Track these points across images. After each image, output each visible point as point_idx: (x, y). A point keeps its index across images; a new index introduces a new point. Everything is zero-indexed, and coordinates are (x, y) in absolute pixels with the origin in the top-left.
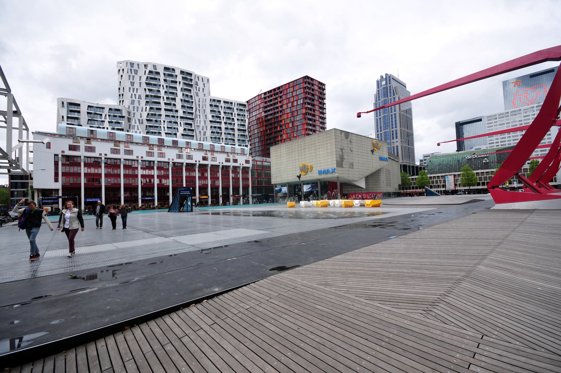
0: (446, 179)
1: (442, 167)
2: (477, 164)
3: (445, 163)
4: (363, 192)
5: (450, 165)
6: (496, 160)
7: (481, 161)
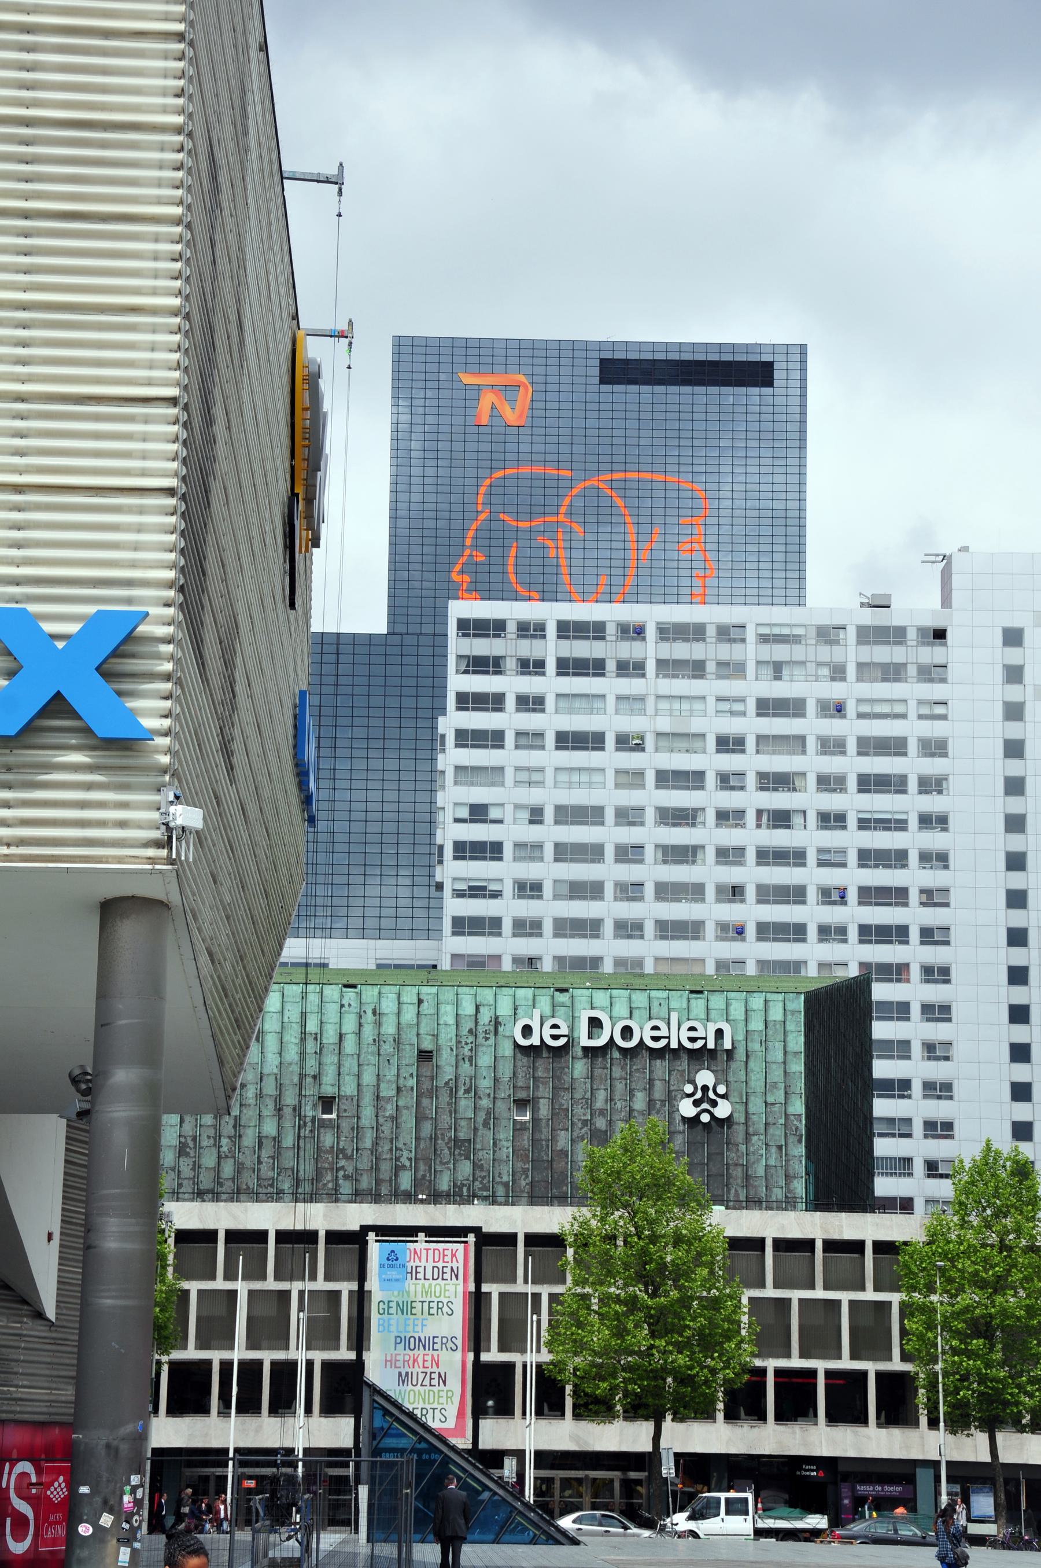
0: (373, 1284)
3: (272, 1061)
6: (798, 1106)
7: (659, 1092)
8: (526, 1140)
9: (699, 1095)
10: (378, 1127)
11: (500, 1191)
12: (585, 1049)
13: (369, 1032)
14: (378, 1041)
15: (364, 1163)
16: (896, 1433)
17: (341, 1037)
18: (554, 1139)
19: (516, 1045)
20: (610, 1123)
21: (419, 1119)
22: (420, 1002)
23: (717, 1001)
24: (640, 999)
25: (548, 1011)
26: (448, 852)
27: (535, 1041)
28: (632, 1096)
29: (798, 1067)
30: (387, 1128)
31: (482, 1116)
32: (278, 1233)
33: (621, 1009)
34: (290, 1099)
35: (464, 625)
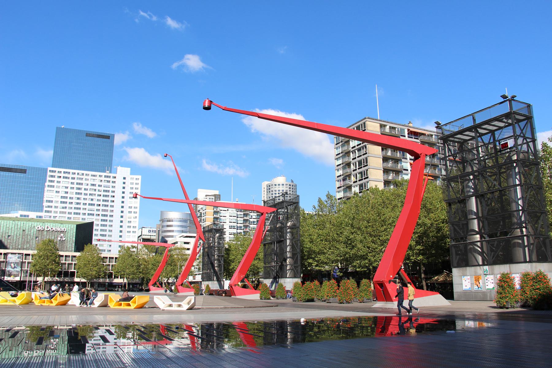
8: (37, 242)
11: (33, 248)
13: (16, 227)
14: (17, 228)
15: (14, 244)
21: (22, 239)
23: (65, 225)
24: (54, 224)
25: (41, 226)
26: (45, 201)
29: (75, 234)
30: (17, 240)
31: (31, 239)
33: (52, 226)
35: (50, 171)
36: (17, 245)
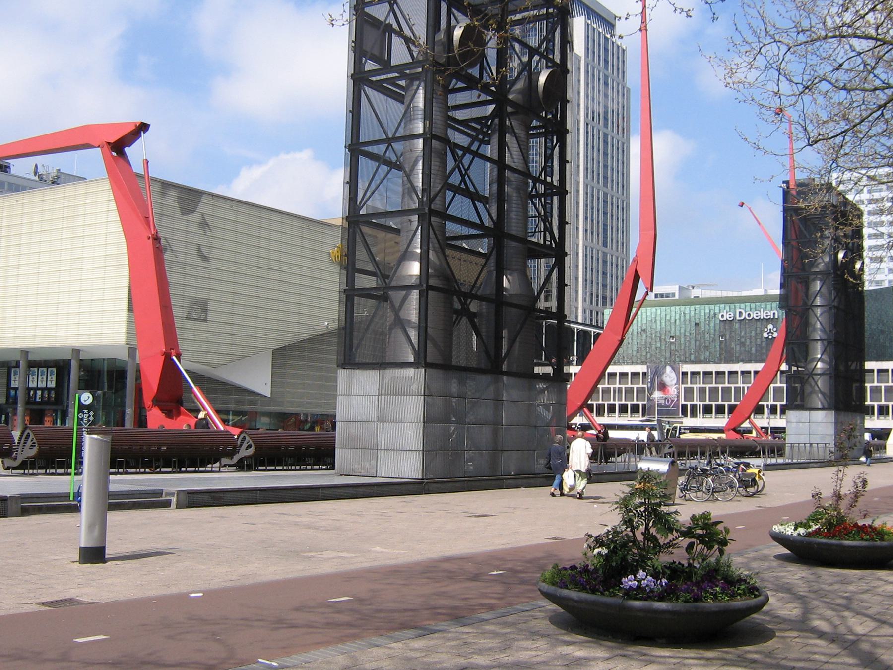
1: (649, 340)
2: (748, 341)
3: (659, 327)
4: (260, 408)
5: (672, 337)
8: (723, 345)
9: (769, 331)
10: (685, 344)
11: (717, 360)
12: (738, 320)
16: (693, 419)
17: (675, 320)
18: (730, 345)
19: (720, 321)
20: (745, 340)
22: (695, 310)
24: (753, 305)
25: (728, 310)
27: (725, 319)
28: (751, 332)
31: (711, 339)
32: (620, 373)
33: (748, 309)
34: (663, 337)
36: (687, 355)
